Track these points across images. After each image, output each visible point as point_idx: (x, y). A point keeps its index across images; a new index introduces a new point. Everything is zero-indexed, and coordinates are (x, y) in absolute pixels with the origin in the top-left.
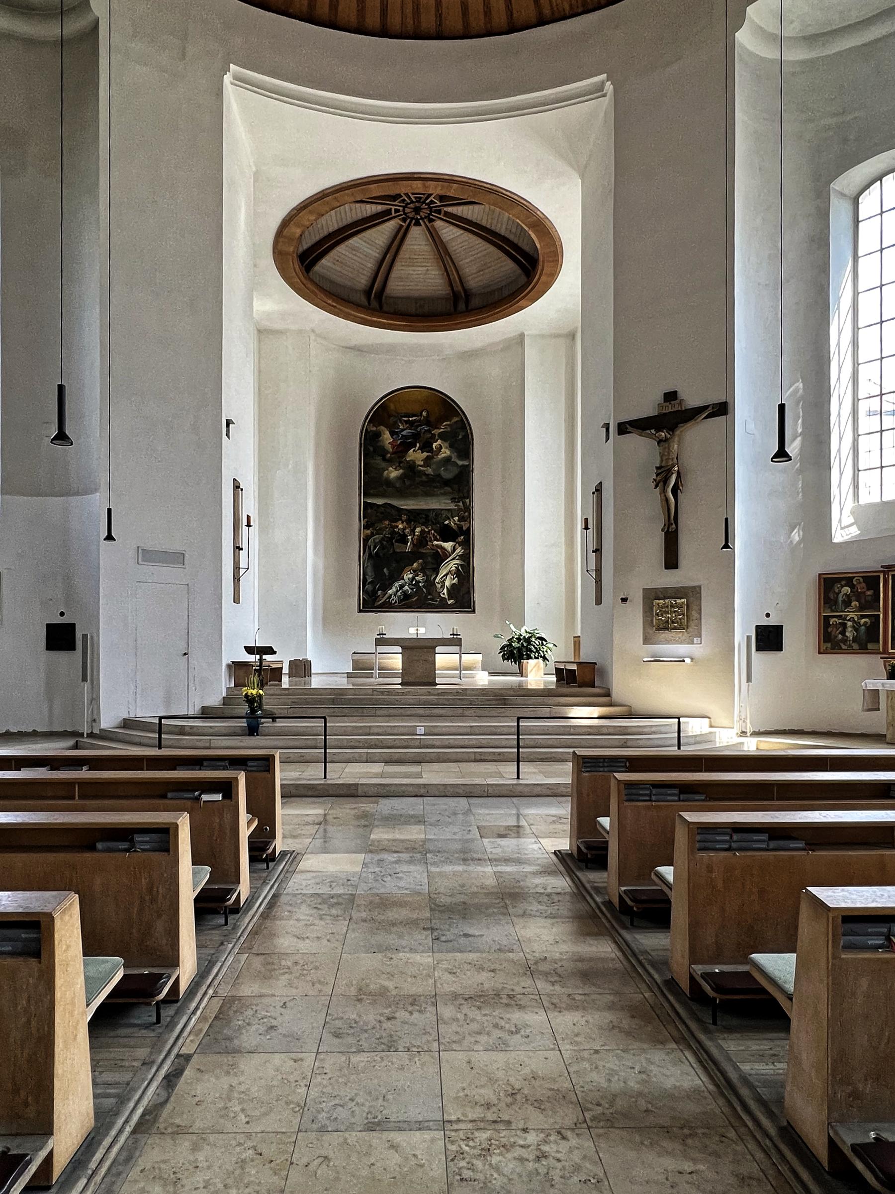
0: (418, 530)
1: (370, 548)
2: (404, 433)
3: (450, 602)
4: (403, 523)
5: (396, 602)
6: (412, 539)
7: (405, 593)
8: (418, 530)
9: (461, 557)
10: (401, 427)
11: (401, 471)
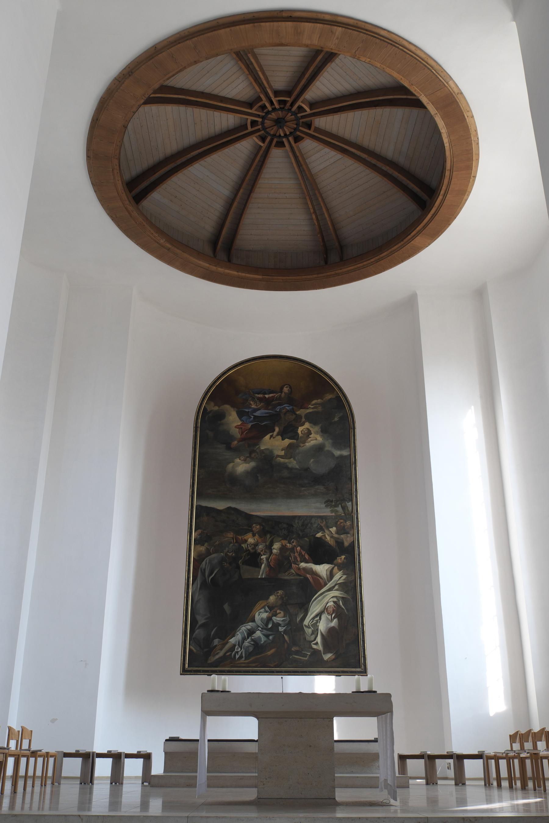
0: (276, 546)
1: (203, 573)
2: (258, 414)
3: (327, 657)
4: (254, 535)
5: (241, 657)
6: (267, 559)
7: (256, 643)
8: (276, 546)
9: (343, 586)
10: (253, 406)
11: (252, 464)
